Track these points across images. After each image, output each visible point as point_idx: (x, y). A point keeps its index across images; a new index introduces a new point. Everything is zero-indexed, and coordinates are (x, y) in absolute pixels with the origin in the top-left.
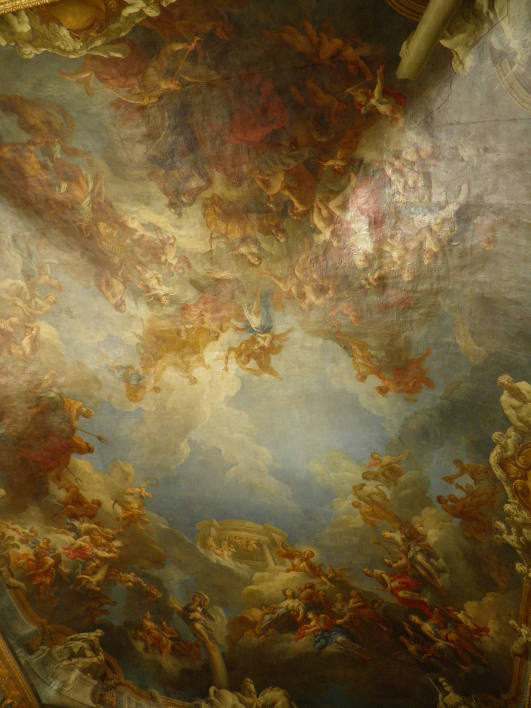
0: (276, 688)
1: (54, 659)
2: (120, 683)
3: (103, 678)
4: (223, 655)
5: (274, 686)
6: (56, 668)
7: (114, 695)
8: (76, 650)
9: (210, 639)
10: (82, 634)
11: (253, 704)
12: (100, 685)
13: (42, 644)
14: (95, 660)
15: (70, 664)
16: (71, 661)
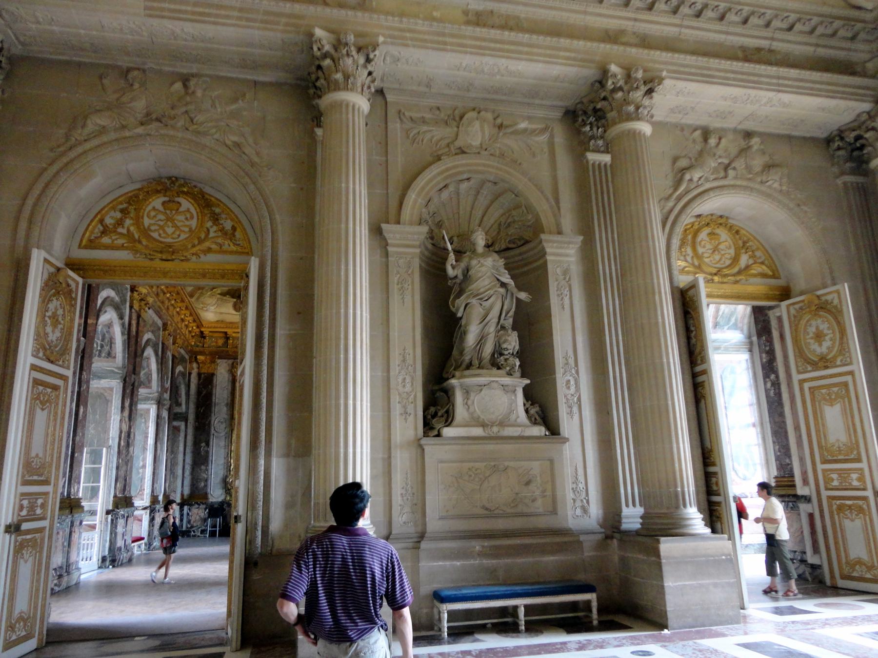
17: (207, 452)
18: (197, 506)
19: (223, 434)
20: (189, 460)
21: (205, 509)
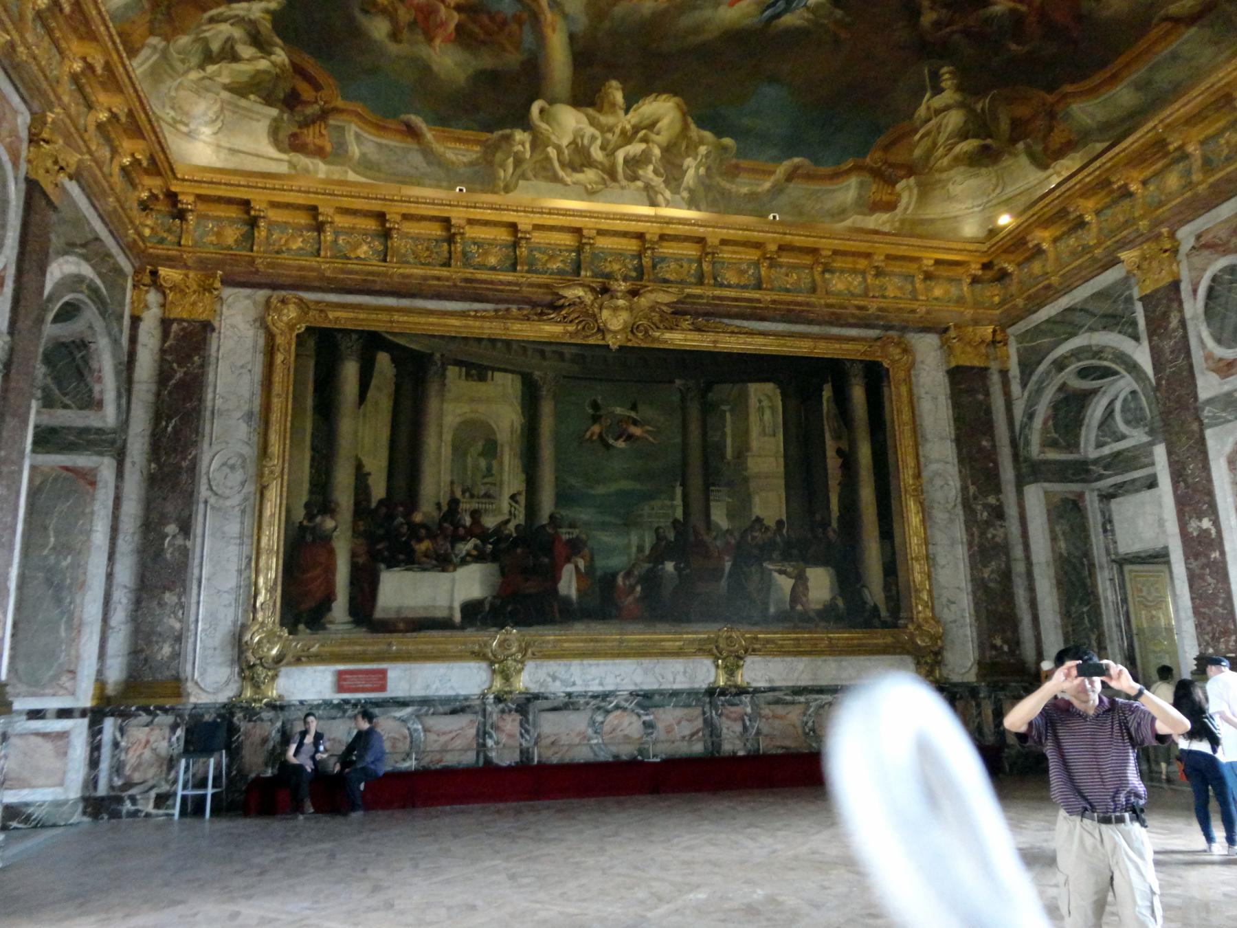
0: (664, 96)
1: (172, 67)
3: (291, 101)
4: (572, 37)
5: (660, 92)
6: (177, 89)
7: (324, 132)
8: (215, 47)
9: (550, 6)
10: (235, 6)
11: (615, 125)
12: (285, 116)
13: (152, 33)
14: (263, 64)
15: (203, 78)
16: (204, 70)
17: (185, 553)
18: (145, 718)
19: (236, 500)
20: (125, 573)
21: (174, 728)
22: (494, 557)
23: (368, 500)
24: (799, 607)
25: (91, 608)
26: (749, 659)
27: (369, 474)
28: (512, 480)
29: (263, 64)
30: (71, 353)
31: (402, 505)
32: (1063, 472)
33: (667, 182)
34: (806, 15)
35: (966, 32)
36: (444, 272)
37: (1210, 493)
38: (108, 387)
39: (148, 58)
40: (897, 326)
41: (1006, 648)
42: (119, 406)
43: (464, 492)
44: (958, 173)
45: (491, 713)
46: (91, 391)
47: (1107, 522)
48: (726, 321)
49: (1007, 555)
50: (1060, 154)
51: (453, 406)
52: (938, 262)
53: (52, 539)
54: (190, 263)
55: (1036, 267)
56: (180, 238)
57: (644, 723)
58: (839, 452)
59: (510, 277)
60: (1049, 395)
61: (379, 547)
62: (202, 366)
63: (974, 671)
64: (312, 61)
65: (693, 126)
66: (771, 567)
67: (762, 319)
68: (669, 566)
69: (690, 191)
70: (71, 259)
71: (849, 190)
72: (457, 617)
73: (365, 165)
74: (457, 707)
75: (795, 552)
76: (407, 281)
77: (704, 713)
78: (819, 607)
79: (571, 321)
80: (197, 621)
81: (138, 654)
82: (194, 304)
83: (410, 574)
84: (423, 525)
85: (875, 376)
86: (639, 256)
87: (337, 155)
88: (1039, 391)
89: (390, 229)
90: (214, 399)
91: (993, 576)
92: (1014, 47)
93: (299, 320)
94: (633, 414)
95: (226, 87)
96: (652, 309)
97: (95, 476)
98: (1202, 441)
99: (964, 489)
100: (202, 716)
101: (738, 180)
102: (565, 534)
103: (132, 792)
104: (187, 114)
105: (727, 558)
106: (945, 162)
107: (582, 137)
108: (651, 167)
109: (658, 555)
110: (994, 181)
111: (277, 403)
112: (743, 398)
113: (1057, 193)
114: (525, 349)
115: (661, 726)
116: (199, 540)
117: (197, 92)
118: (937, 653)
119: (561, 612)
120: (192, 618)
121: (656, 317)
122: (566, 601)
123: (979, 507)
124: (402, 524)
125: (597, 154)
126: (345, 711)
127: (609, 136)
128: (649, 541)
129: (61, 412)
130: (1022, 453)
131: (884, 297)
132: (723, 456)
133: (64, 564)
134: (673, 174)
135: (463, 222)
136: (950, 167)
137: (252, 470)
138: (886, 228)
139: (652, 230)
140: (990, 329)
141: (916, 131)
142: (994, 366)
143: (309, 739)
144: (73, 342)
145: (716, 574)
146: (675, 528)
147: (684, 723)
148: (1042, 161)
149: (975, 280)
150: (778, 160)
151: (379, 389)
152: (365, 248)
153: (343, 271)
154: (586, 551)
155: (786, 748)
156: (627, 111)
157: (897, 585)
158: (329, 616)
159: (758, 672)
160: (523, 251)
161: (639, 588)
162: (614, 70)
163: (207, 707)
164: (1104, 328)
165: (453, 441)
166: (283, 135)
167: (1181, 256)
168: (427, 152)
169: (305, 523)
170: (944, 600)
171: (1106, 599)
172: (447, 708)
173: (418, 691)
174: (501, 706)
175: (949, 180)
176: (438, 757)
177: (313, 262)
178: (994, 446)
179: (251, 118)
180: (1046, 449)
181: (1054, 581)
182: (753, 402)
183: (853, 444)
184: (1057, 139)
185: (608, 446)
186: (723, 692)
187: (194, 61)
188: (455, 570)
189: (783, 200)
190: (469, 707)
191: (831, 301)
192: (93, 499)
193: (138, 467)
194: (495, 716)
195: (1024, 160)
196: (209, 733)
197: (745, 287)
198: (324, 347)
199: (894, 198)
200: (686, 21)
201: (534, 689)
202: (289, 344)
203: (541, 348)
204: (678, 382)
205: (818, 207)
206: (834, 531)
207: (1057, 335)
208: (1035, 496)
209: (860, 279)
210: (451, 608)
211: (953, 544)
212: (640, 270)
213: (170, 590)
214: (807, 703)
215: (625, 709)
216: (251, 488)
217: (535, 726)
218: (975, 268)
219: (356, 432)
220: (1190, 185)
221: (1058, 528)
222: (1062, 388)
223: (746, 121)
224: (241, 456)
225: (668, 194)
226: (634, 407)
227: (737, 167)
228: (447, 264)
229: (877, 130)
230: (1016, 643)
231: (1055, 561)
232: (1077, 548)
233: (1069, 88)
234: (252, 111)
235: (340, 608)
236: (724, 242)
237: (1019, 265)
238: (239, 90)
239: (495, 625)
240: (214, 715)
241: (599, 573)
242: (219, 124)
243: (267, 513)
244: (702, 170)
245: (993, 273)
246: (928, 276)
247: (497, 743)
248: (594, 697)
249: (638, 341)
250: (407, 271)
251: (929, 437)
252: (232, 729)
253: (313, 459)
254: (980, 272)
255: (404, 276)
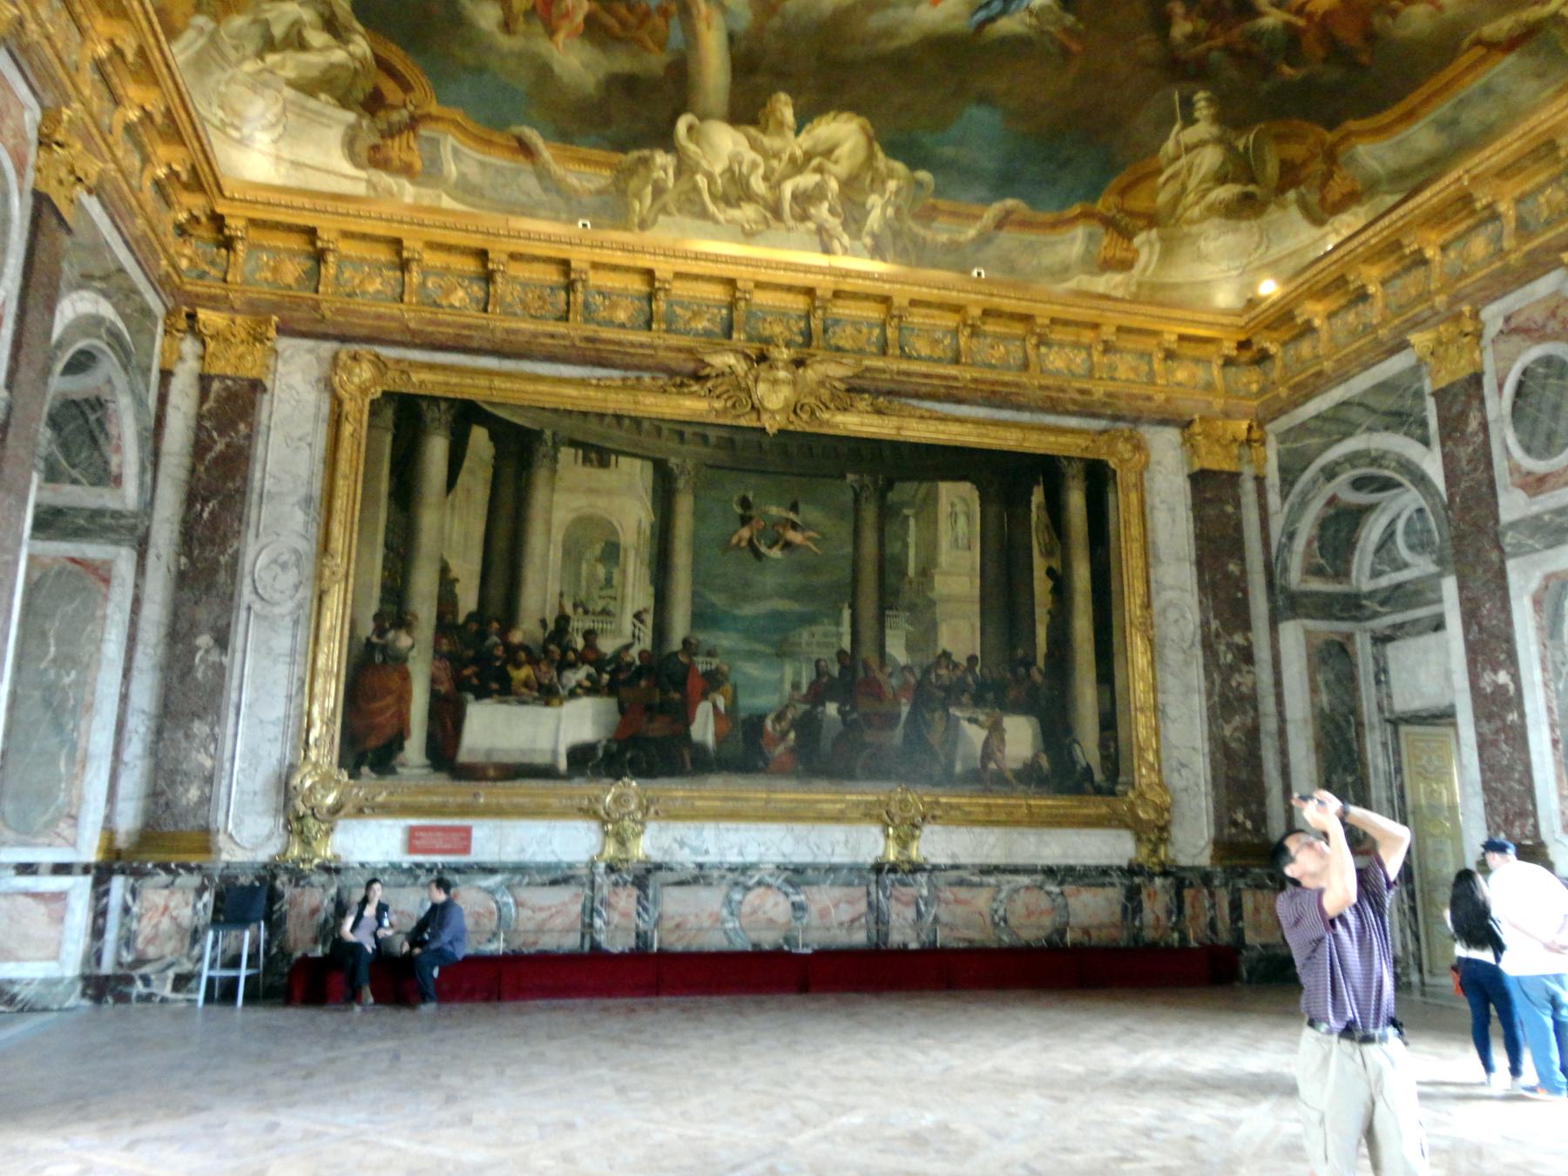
1: (223, 56)
2: (429, 117)
3: (373, 104)
4: (731, 38)
5: (842, 108)
6: (227, 84)
7: (412, 144)
8: (278, 31)
12: (365, 123)
14: (339, 55)
15: (261, 71)
16: (262, 59)
17: (220, 671)
18: (163, 877)
19: (290, 605)
21: (200, 892)
22: (612, 690)
23: (455, 614)
24: (992, 766)
25: (100, 738)
26: (927, 830)
27: (457, 580)
28: (637, 593)
29: (339, 55)
30: (83, 413)
31: (498, 621)
32: (1325, 607)
33: (845, 225)
34: (1028, 20)
35: (1229, 49)
36: (561, 328)
37: (1509, 640)
38: (128, 458)
39: (191, 44)
40: (1128, 416)
41: (1249, 825)
42: (142, 484)
43: (575, 606)
44: (1211, 226)
45: (601, 887)
46: (106, 463)
47: (1381, 672)
48: (914, 402)
49: (1256, 709)
50: (1338, 207)
51: (566, 498)
52: (1182, 338)
53: (52, 649)
54: (237, 304)
55: (1305, 348)
56: (226, 273)
57: (793, 904)
58: (1050, 572)
59: (642, 337)
60: (1315, 509)
61: (467, 672)
62: (249, 437)
63: (1208, 852)
64: (402, 53)
65: (880, 155)
66: (958, 714)
67: (959, 401)
68: (832, 709)
69: (874, 236)
70: (86, 294)
71: (1074, 243)
72: (563, 764)
73: (464, 189)
74: (560, 877)
75: (990, 696)
76: (512, 337)
77: (869, 894)
78: (1017, 765)
79: (718, 397)
80: (233, 758)
81: (157, 796)
82: (241, 357)
83: (504, 708)
84: (523, 647)
85: (1098, 477)
86: (807, 316)
87: (428, 174)
88: (1303, 503)
89: (493, 271)
90: (263, 478)
91: (1237, 734)
92: (1287, 70)
93: (375, 382)
94: (792, 516)
95: (291, 84)
96: (821, 383)
97: (110, 570)
98: (1502, 574)
99: (1205, 624)
100: (237, 878)
101: (935, 225)
102: (702, 664)
103: (145, 970)
104: (238, 115)
105: (904, 701)
106: (1196, 211)
107: (740, 164)
108: (825, 205)
109: (817, 695)
110: (1256, 238)
111: (342, 486)
112: (932, 499)
113: (1335, 256)
114: (659, 430)
115: (814, 909)
116: (238, 656)
117: (254, 89)
118: (1163, 829)
119: (693, 761)
120: (227, 754)
121: (825, 394)
122: (701, 748)
123: (1222, 648)
124: (496, 645)
125: (758, 185)
126: (417, 877)
127: (775, 163)
128: (807, 676)
129: (67, 488)
130: (1278, 581)
131: (1113, 379)
132: (903, 573)
133: (67, 680)
134: (853, 216)
135: (586, 266)
136: (1202, 219)
137: (309, 569)
138: (1119, 293)
139: (825, 285)
140: (1244, 425)
141: (1160, 171)
142: (1248, 471)
143: (370, 911)
144: (86, 401)
145: (891, 720)
146: (840, 660)
147: (843, 906)
148: (1318, 215)
149: (1228, 362)
150: (987, 202)
151: (472, 472)
152: (460, 293)
153: (431, 322)
154: (728, 687)
155: (970, 941)
156: (798, 132)
157: (1116, 740)
158: (401, 757)
159: (937, 845)
160: (660, 306)
161: (792, 735)
162: (783, 78)
163: (241, 865)
164: (1387, 428)
165: (564, 541)
166: (362, 148)
167: (1486, 341)
168: (543, 175)
169: (375, 639)
170: (1174, 764)
171: (1376, 768)
172: (546, 878)
173: (510, 855)
174: (613, 877)
175: (1200, 235)
176: (531, 938)
177: (395, 309)
178: (1244, 572)
179: (321, 124)
180: (1310, 578)
181: (1312, 743)
182: (944, 507)
183: (1067, 563)
184: (1336, 189)
185: (758, 555)
186: (894, 869)
187: (250, 48)
188: (561, 703)
189: (990, 252)
190: (573, 877)
191: (1050, 381)
192: (106, 598)
193: (164, 558)
194: (605, 891)
195: (1294, 213)
196: (244, 900)
197: (939, 361)
198: (405, 415)
199: (1129, 255)
200: (876, 21)
201: (657, 857)
202: (361, 412)
203: (680, 429)
204: (850, 477)
205: (1035, 262)
206: (1040, 671)
207: (1329, 435)
208: (1293, 635)
209: (1084, 355)
210: (555, 753)
211: (1187, 690)
212: (808, 336)
213: (199, 717)
214: (998, 888)
215: (769, 886)
216: (306, 592)
217: (656, 902)
218: (1229, 348)
219: (442, 528)
220: (1500, 253)
221: (1320, 678)
222: (1332, 501)
223: (948, 151)
224: (296, 551)
225: (846, 239)
226: (794, 508)
227: (934, 208)
228: (564, 318)
229: (1109, 168)
230: (1260, 819)
231: (1314, 717)
232: (1344, 703)
233: (1352, 125)
234: (323, 114)
235: (414, 748)
236: (914, 303)
237: (1284, 344)
238: (308, 87)
239: (609, 775)
240: (251, 877)
241: (743, 715)
242: (280, 129)
243: (326, 624)
244: (890, 211)
245: (1249, 353)
246: (1170, 355)
247: (607, 923)
248: (732, 869)
249: (799, 425)
250: (514, 325)
251: (1163, 557)
252: (274, 896)
253: (386, 559)
254: (1235, 353)
255: (508, 331)
